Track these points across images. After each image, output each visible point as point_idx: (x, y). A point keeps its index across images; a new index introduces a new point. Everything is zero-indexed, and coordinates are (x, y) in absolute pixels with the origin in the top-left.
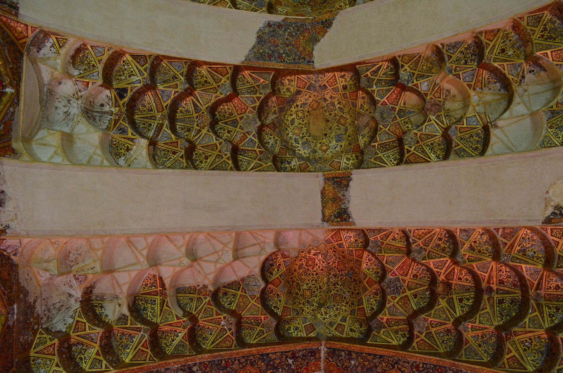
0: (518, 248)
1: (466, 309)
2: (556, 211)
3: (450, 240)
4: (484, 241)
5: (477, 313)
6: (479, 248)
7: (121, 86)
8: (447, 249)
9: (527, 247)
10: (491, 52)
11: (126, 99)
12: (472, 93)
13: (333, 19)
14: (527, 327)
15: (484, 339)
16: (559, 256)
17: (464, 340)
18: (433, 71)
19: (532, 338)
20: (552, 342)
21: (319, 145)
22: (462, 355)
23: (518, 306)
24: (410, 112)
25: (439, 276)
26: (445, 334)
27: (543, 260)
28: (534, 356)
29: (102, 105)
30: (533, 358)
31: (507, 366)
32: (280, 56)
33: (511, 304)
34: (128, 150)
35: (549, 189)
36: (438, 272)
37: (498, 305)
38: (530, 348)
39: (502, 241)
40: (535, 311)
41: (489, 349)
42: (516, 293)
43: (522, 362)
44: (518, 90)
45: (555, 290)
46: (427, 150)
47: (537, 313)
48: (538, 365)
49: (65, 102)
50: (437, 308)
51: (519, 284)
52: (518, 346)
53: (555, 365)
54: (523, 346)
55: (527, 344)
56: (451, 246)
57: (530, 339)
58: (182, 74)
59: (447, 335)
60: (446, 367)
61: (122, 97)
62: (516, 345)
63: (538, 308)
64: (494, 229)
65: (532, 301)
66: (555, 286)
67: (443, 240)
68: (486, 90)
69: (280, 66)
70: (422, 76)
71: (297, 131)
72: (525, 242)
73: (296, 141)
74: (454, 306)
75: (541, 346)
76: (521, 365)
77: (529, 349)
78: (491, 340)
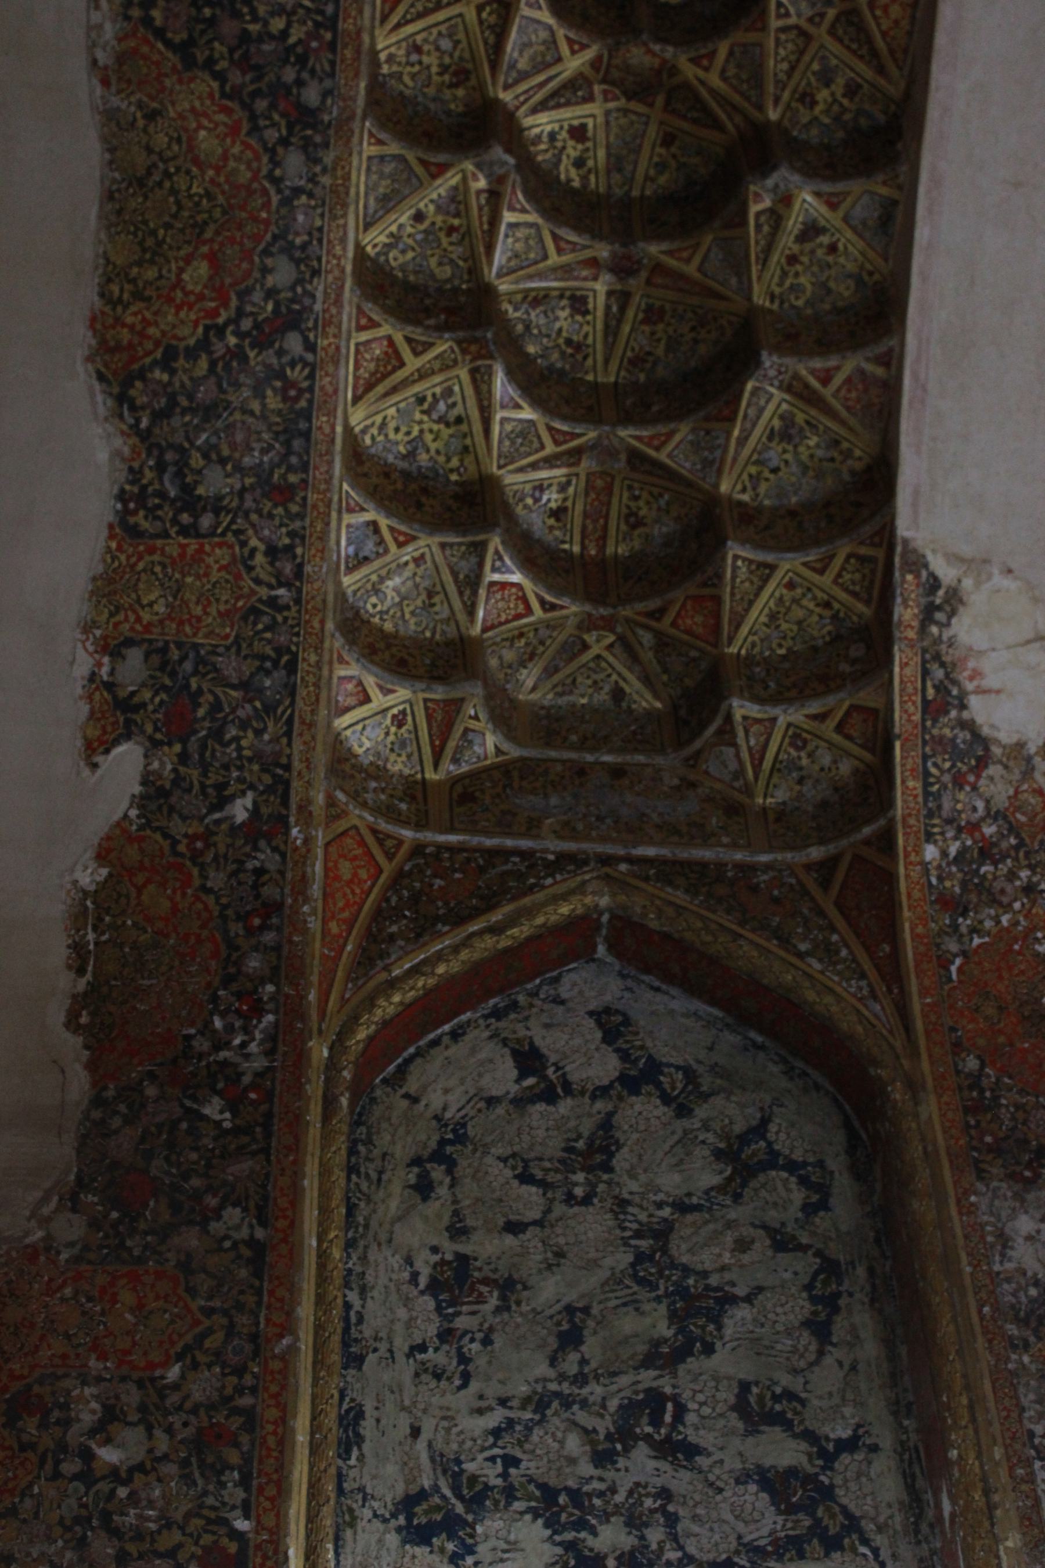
0: (800, 418)
1: (542, 154)
2: (941, 593)
3: (840, 134)
4: (832, 284)
5: (543, 212)
6: (805, 259)
8: (805, 116)
9: (801, 449)
14: (506, 414)
15: (442, 235)
16: (773, 568)
17: (441, 158)
19: (464, 427)
20: (456, 497)
22: (380, 142)
23: (559, 365)
25: (695, 61)
26: (447, 60)
27: (745, 497)
28: (397, 430)
30: (392, 425)
31: (364, 337)
33: (569, 342)
35: (1016, 578)
36: (712, 55)
37: (568, 293)
38: (425, 418)
39: (838, 368)
40: (557, 443)
41: (403, 252)
42: (607, 361)
43: (380, 389)
45: (625, 510)
47: (550, 448)
48: (368, 441)
50: (561, 33)
51: (642, 377)
52: (437, 379)
53: (389, 514)
54: (434, 395)
55: (442, 406)
56: (814, 132)
57: (459, 420)
59: (444, 69)
60: (332, 75)
62: (441, 370)
63: (569, 453)
64: (891, 350)
65: (592, 435)
66: (642, 513)
67: (845, 102)
72: (818, 446)
74: (558, 106)
75: (433, 452)
76: (370, 387)
77: (423, 412)
78: (440, 264)
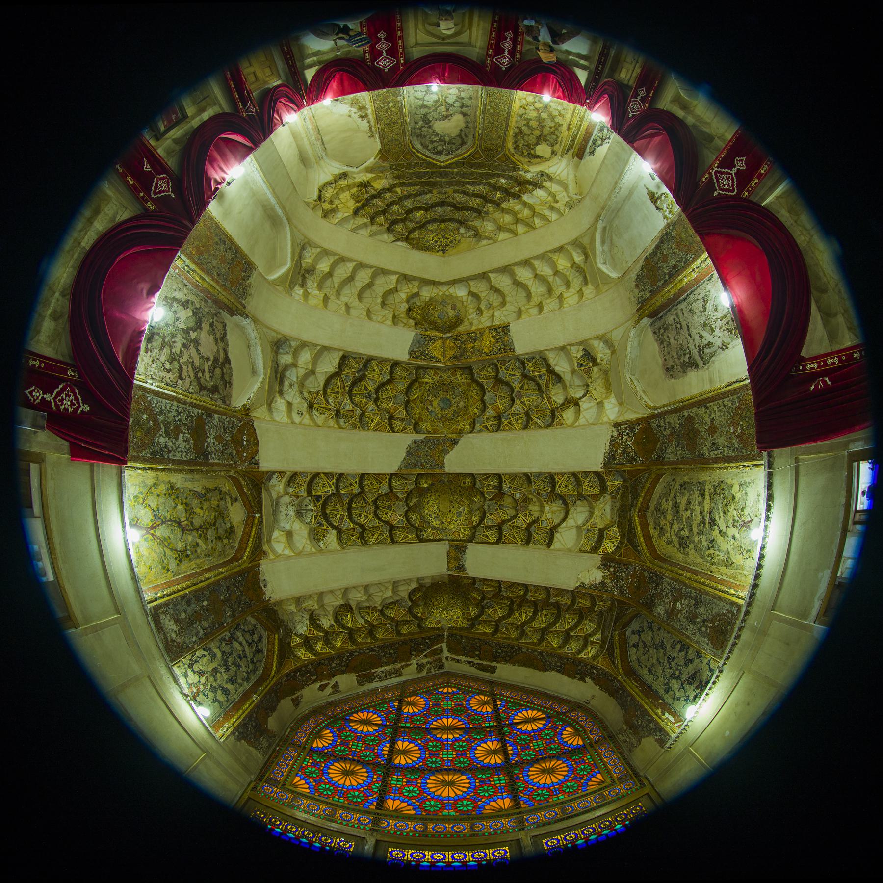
7: (317, 494)
10: (559, 486)
11: (321, 502)
12: (546, 505)
13: (460, 439)
18: (524, 486)
21: (445, 518)
24: (507, 507)
29: (306, 505)
32: (422, 465)
34: (324, 536)
44: (572, 509)
46: (516, 535)
49: (285, 507)
58: (356, 482)
61: (318, 501)
68: (554, 504)
69: (422, 472)
70: (517, 489)
71: (431, 509)
73: (430, 516)
